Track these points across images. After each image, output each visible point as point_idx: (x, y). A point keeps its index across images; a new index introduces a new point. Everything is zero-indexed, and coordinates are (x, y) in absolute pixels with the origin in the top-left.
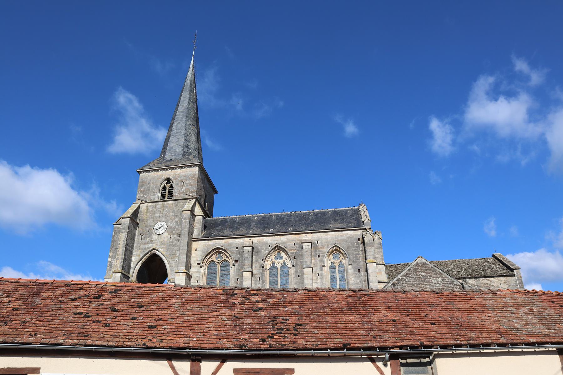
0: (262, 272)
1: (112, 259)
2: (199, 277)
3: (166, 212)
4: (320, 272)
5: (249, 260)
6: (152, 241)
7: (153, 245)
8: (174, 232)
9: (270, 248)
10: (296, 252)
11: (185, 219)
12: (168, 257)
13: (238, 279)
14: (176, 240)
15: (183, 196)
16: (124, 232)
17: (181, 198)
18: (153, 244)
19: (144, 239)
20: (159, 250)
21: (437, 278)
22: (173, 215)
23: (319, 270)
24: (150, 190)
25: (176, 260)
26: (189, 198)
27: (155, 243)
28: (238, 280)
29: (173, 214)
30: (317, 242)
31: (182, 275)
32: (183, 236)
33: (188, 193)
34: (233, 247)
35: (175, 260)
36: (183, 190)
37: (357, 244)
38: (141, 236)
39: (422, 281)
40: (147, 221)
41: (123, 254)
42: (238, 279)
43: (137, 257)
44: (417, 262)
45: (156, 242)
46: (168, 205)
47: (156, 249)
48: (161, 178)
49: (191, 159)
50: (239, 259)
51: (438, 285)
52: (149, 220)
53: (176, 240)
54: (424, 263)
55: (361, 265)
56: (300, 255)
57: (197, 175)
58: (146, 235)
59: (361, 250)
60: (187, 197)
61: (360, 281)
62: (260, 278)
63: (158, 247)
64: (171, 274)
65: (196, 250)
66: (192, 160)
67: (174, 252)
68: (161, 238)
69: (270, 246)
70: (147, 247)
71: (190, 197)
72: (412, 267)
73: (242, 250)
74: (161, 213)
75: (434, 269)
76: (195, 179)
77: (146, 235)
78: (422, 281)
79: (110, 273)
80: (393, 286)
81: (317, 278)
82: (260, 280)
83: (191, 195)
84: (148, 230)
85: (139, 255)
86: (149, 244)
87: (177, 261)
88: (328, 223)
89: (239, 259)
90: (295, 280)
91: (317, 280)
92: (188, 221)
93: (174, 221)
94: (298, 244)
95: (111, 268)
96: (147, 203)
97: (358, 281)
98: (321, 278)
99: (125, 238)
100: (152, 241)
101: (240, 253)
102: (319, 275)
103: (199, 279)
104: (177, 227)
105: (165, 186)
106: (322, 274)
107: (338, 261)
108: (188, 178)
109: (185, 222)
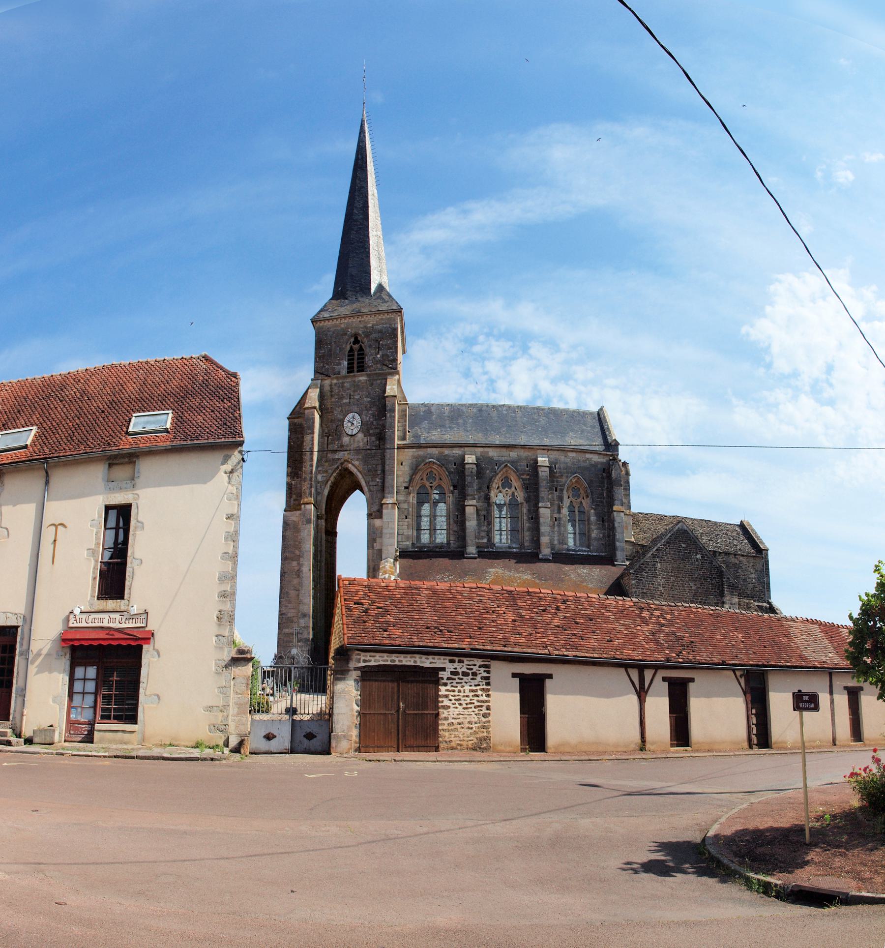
4: (558, 515)
7: (344, 454)
8: (371, 431)
9: (496, 467)
12: (366, 476)
19: (332, 443)
22: (368, 402)
23: (556, 511)
25: (378, 480)
35: (376, 481)
47: (350, 460)
58: (333, 436)
61: (603, 536)
63: (353, 457)
65: (402, 465)
70: (337, 457)
81: (554, 525)
85: (327, 472)
91: (554, 528)
93: (371, 412)
98: (559, 525)
100: (342, 446)
102: (556, 520)
106: (560, 519)
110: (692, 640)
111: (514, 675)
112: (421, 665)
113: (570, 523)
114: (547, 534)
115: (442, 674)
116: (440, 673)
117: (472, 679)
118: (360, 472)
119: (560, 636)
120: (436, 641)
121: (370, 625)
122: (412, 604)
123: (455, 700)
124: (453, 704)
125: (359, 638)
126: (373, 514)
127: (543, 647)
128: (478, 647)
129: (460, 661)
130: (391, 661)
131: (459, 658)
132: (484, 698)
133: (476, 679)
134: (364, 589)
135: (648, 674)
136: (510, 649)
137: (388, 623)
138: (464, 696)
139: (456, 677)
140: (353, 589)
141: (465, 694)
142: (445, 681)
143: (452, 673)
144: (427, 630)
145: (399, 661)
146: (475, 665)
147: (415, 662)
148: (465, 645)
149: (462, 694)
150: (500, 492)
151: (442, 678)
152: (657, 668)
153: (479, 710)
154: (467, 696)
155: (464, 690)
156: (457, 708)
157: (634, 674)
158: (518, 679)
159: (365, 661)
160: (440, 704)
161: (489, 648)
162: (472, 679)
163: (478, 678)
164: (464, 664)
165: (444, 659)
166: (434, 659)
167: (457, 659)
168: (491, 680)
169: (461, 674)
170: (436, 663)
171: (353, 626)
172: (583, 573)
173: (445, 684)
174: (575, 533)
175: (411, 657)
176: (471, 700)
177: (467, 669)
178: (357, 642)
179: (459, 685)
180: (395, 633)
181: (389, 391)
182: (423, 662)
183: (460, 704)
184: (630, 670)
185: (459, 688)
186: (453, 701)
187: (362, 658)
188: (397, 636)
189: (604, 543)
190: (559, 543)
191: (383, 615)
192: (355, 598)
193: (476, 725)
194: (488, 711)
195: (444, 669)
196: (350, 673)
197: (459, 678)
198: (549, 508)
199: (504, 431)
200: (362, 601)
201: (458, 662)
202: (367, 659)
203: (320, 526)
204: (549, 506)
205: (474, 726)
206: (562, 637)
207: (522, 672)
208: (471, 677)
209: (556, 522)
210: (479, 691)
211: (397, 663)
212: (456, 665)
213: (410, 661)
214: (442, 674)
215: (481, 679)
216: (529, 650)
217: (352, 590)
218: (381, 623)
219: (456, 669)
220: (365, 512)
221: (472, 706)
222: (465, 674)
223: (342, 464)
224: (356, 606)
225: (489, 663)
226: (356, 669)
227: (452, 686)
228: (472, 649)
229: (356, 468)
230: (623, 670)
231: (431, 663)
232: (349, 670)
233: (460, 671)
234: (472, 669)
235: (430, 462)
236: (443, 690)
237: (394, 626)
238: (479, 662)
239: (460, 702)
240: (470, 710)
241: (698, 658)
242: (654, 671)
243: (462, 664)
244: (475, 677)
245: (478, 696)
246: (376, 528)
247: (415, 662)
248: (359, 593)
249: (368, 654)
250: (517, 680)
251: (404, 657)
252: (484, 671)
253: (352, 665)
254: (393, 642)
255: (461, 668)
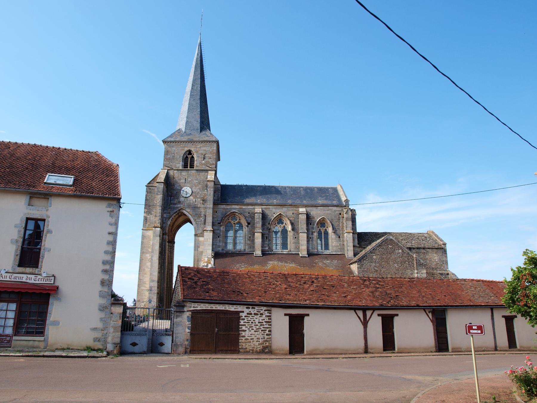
0: (269, 233)
1: (146, 214)
2: (220, 233)
3: (191, 180)
5: (260, 224)
6: (180, 202)
10: (294, 220)
11: (210, 187)
13: (250, 237)
14: (201, 203)
15: (204, 167)
16: (160, 194)
17: (202, 169)
18: (181, 204)
20: (186, 210)
21: (399, 249)
22: (196, 182)
24: (175, 159)
25: (201, 219)
26: (209, 169)
27: (182, 204)
28: (250, 238)
29: (197, 181)
30: (310, 213)
31: (210, 232)
32: (208, 202)
33: (209, 165)
34: (246, 212)
35: (200, 219)
36: (203, 162)
37: (339, 218)
38: (170, 197)
39: (389, 251)
40: (174, 185)
41: (160, 212)
42: (250, 237)
43: (168, 214)
44: (387, 238)
45: (183, 203)
46: (191, 174)
47: (184, 209)
48: (183, 150)
49: (209, 136)
50: (251, 222)
51: (399, 254)
52: (176, 185)
53: (201, 203)
54: (391, 239)
55: (341, 233)
56: (297, 222)
57: (215, 150)
59: (341, 222)
60: (207, 168)
61: (340, 245)
62: (267, 237)
64: (198, 230)
65: (216, 212)
66: (210, 136)
67: (199, 212)
68: (187, 200)
69: (274, 213)
71: (211, 169)
72: (383, 241)
73: (253, 215)
74: (186, 180)
75: (397, 244)
76: (214, 154)
77: (174, 197)
78: (389, 251)
79: (146, 225)
80: (371, 253)
82: (267, 239)
83: (211, 167)
84: (175, 193)
85: (169, 213)
86: (177, 204)
87: (201, 220)
88: (316, 198)
89: (251, 222)
90: (293, 241)
92: (212, 189)
94: (295, 213)
95: (146, 222)
96: (173, 170)
97: (338, 245)
99: (161, 200)
100: (179, 202)
101: (251, 217)
103: (220, 235)
104: (200, 192)
105: (187, 156)
107: (324, 228)
108: (207, 152)
109: (210, 190)
110: (397, 294)
111: (286, 315)
112: (229, 310)
113: (319, 240)
114: (305, 245)
115: (241, 314)
116: (240, 313)
117: (260, 317)
118: (191, 215)
119: (314, 295)
120: (238, 298)
121: (198, 289)
122: (224, 280)
123: (250, 327)
124: (248, 329)
125: (191, 296)
126: (198, 234)
127: (304, 301)
128: (263, 301)
129: (252, 308)
130: (210, 307)
131: (252, 307)
132: (267, 326)
133: (262, 317)
134: (194, 272)
135: (369, 313)
136: (283, 302)
137: (209, 289)
138: (255, 325)
139: (250, 316)
140: (187, 272)
141: (255, 324)
142: (243, 317)
143: (248, 314)
144: (233, 293)
145: (215, 307)
146: (262, 310)
147: (225, 308)
148: (256, 300)
149: (254, 324)
150: (276, 226)
151: (242, 316)
152: (374, 309)
153: (263, 332)
154: (257, 325)
155: (255, 323)
156: (250, 331)
157: (360, 313)
158: (288, 317)
159: (194, 307)
160: (240, 329)
161: (271, 301)
162: (260, 317)
163: (264, 316)
164: (255, 309)
165: (243, 307)
166: (237, 307)
167: (251, 307)
168: (273, 317)
169: (253, 314)
170: (238, 309)
171: (187, 290)
172: (327, 262)
173: (244, 319)
174: (322, 244)
175: (223, 306)
176: (259, 327)
177: (257, 312)
178: (190, 298)
179: (252, 320)
180: (213, 294)
181: (209, 178)
182: (230, 308)
183: (252, 329)
184: (358, 312)
185: (252, 321)
186: (249, 328)
187: (193, 306)
188: (214, 295)
189: (340, 248)
190: (312, 249)
191: (206, 285)
192: (188, 276)
193: (262, 340)
194: (270, 333)
195: (243, 312)
196: (185, 313)
197: (252, 316)
198: (307, 233)
199: (279, 198)
200: (193, 278)
201: (252, 308)
202: (195, 306)
203: (164, 239)
204: (307, 232)
205: (260, 340)
206: (315, 295)
207: (290, 313)
208: (259, 315)
209: (310, 239)
210: (264, 322)
211: (214, 308)
212: (250, 310)
213: (222, 308)
214: (241, 314)
215: (266, 316)
216: (295, 303)
217: (186, 272)
218: (205, 289)
219: (250, 311)
220: (194, 233)
221: (260, 330)
222: (255, 314)
223: (180, 210)
224: (189, 280)
225: (271, 309)
226: (188, 311)
227: (247, 320)
228: (260, 302)
229: (188, 212)
230: (353, 311)
231: (235, 309)
232: (184, 312)
233: (253, 313)
234: (260, 312)
235: (235, 212)
236: (242, 322)
237: (213, 290)
238: (265, 308)
239: (252, 328)
240: (259, 332)
241: (401, 304)
242: (372, 311)
243: (254, 309)
244: (262, 316)
245: (264, 325)
246: (200, 241)
247: (225, 308)
248: (191, 274)
249: (196, 304)
250: (287, 317)
251: (219, 306)
252: (268, 313)
253: (185, 309)
254: (212, 298)
255: (253, 311)
